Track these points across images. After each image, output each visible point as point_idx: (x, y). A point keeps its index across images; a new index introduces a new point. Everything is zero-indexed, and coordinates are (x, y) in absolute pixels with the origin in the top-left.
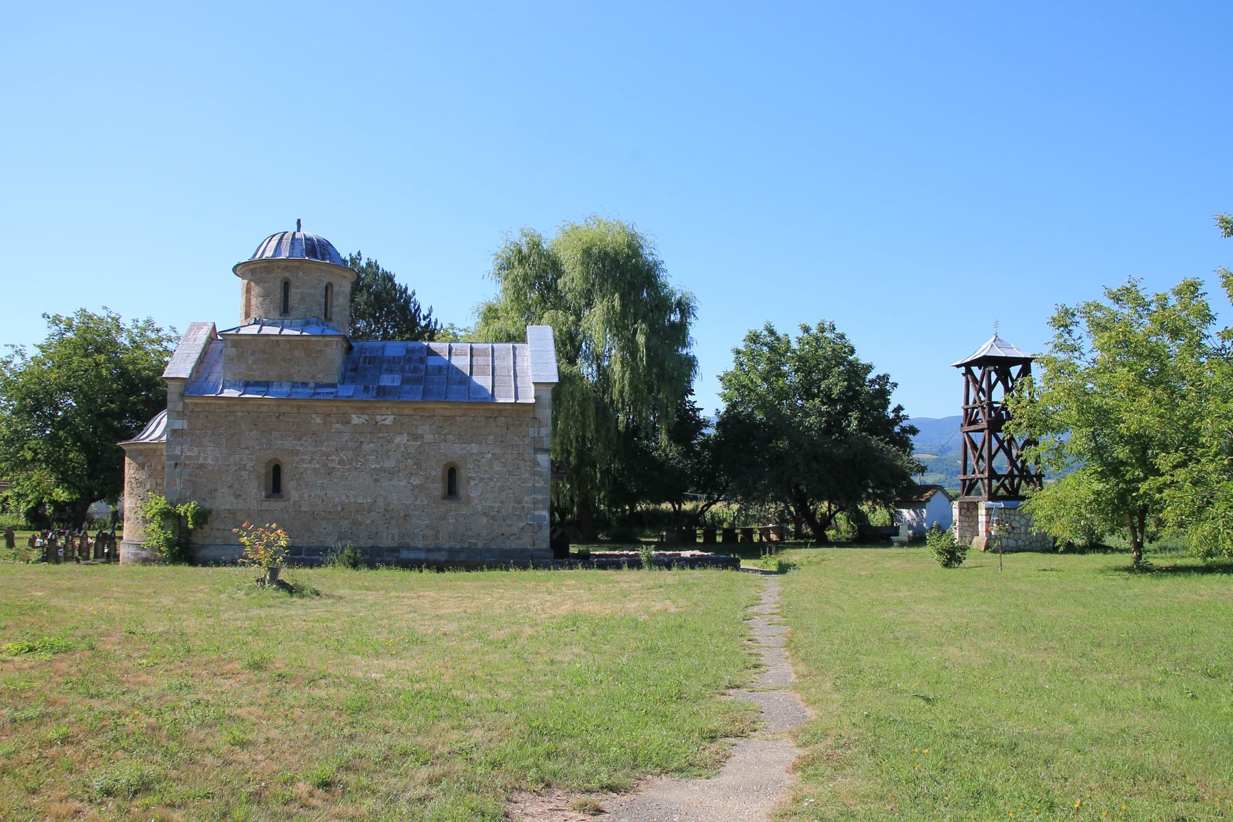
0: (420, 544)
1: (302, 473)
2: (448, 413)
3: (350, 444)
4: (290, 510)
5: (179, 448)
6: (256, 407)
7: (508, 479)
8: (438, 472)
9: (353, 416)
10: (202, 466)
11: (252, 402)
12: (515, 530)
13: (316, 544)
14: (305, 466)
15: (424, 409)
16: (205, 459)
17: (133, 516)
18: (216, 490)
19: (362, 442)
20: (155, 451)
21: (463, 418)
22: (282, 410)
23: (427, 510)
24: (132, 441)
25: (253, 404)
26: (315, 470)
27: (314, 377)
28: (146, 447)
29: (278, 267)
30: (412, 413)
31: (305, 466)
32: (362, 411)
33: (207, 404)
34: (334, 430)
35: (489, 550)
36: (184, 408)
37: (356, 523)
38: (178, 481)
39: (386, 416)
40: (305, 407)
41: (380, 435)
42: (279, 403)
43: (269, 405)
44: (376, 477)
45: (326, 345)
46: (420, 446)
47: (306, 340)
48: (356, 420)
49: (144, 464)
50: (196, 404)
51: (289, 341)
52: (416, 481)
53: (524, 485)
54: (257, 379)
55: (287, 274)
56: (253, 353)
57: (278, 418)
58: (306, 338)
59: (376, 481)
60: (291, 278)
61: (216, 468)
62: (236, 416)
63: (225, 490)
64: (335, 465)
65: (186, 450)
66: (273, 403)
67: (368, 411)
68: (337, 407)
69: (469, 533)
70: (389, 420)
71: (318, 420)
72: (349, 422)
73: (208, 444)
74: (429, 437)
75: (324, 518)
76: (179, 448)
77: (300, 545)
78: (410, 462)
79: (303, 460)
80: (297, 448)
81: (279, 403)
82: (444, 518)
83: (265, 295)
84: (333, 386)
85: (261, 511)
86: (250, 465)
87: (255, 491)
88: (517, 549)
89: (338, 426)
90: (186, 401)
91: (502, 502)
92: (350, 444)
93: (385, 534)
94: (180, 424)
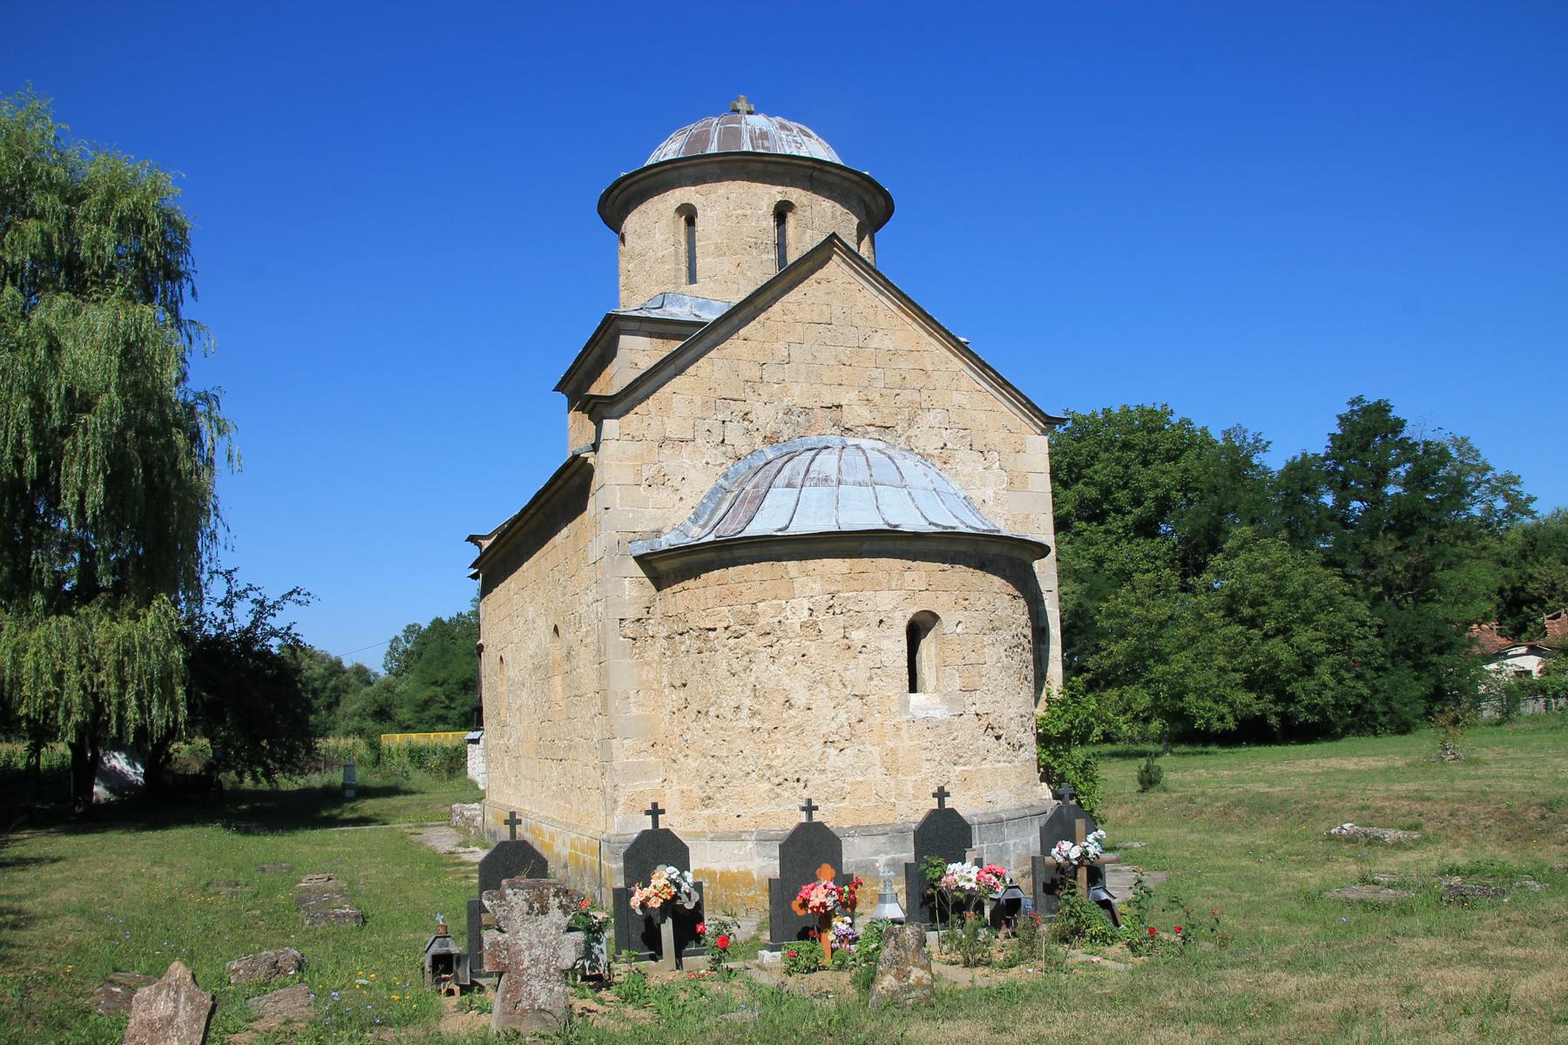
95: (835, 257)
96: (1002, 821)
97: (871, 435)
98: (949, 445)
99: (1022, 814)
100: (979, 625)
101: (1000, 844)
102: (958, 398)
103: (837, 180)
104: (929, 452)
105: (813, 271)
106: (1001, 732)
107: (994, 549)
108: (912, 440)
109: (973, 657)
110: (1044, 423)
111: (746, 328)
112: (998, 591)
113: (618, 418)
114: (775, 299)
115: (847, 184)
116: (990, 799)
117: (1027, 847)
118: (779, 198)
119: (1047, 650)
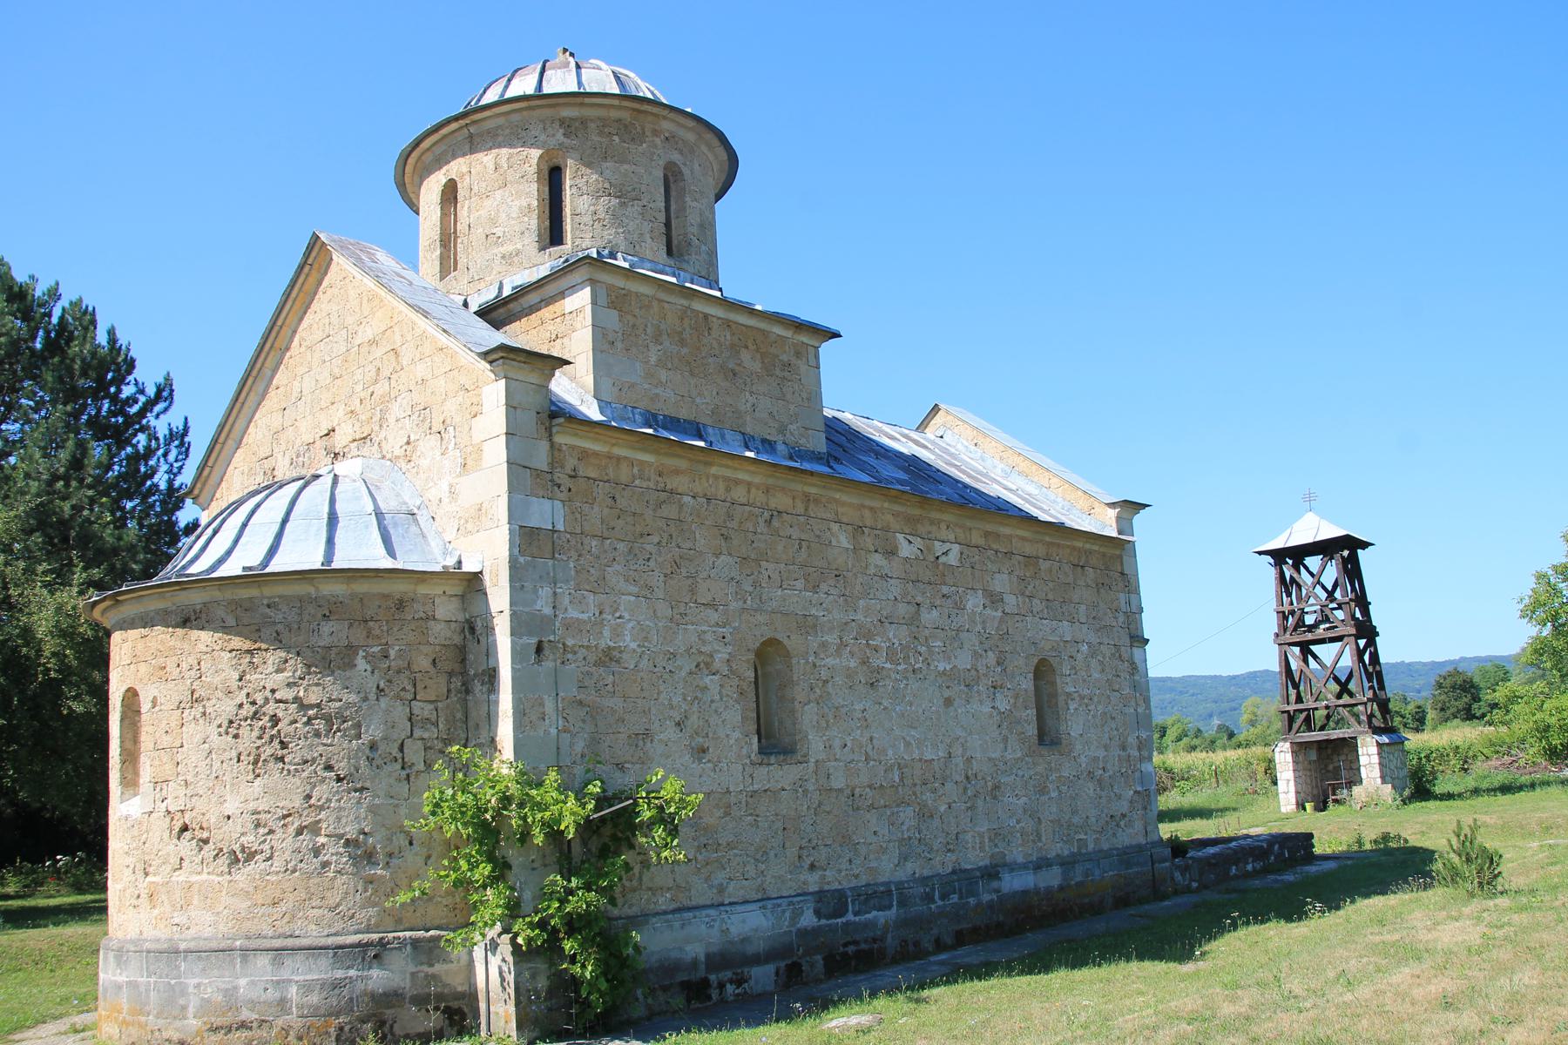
0: (1017, 854)
1: (826, 682)
2: (1029, 549)
3: (903, 609)
4: (811, 788)
5: (545, 592)
6: (722, 486)
7: (1109, 697)
8: (1027, 684)
9: (900, 537)
10: (609, 657)
11: (714, 470)
12: (1124, 806)
13: (863, 880)
14: (830, 661)
15: (997, 536)
16: (617, 633)
17: (285, 842)
18: (647, 735)
19: (918, 605)
20: (401, 605)
21: (1048, 563)
22: (772, 505)
23: (1020, 773)
24: (155, 581)
25: (716, 477)
26: (850, 674)
27: (782, 430)
28: (361, 587)
29: (656, 133)
30: (981, 542)
31: (830, 661)
32: (912, 526)
33: (610, 457)
34: (872, 571)
35: (1107, 854)
36: (551, 464)
37: (925, 814)
38: (549, 706)
39: (947, 546)
40: (817, 501)
41: (945, 589)
42: (770, 481)
43: (749, 484)
44: (947, 693)
45: (798, 354)
46: (1001, 621)
47: (763, 331)
48: (906, 550)
49: (352, 649)
50: (584, 455)
51: (728, 324)
52: (1003, 705)
53: (1126, 710)
54: (671, 411)
55: (675, 157)
56: (657, 339)
57: (769, 522)
58: (763, 325)
59: (948, 702)
60: (686, 171)
61: (644, 663)
62: (681, 506)
63: (670, 733)
64: (879, 661)
65: (566, 600)
66: (757, 480)
67: (922, 529)
68: (871, 509)
69: (1076, 820)
70: (953, 559)
71: (844, 540)
72: (891, 552)
73: (622, 585)
74: (1011, 600)
75: (872, 806)
76: (545, 592)
77: (836, 886)
78: (991, 657)
79: (824, 645)
80: (813, 612)
81: (770, 481)
82: (1043, 791)
83: (624, 194)
84: (816, 457)
85: (753, 794)
86: (721, 656)
87: (737, 734)
88: (1131, 846)
89: (878, 559)
90: (559, 439)
91: (1106, 747)
92: (903, 609)
93: (969, 837)
94: (546, 513)
95: (334, 257)
96: (177, 952)
97: (352, 454)
98: (412, 438)
99: (223, 945)
100: (176, 698)
101: (173, 982)
102: (421, 370)
103: (501, 121)
104: (395, 454)
105: (320, 283)
106: (205, 835)
107: (195, 598)
108: (383, 444)
109: (166, 741)
110: (491, 362)
111: (277, 376)
112: (205, 649)
113: (207, 508)
114: (295, 332)
115: (515, 117)
116: (176, 921)
117: (230, 993)
118: (444, 181)
119: (497, 702)
